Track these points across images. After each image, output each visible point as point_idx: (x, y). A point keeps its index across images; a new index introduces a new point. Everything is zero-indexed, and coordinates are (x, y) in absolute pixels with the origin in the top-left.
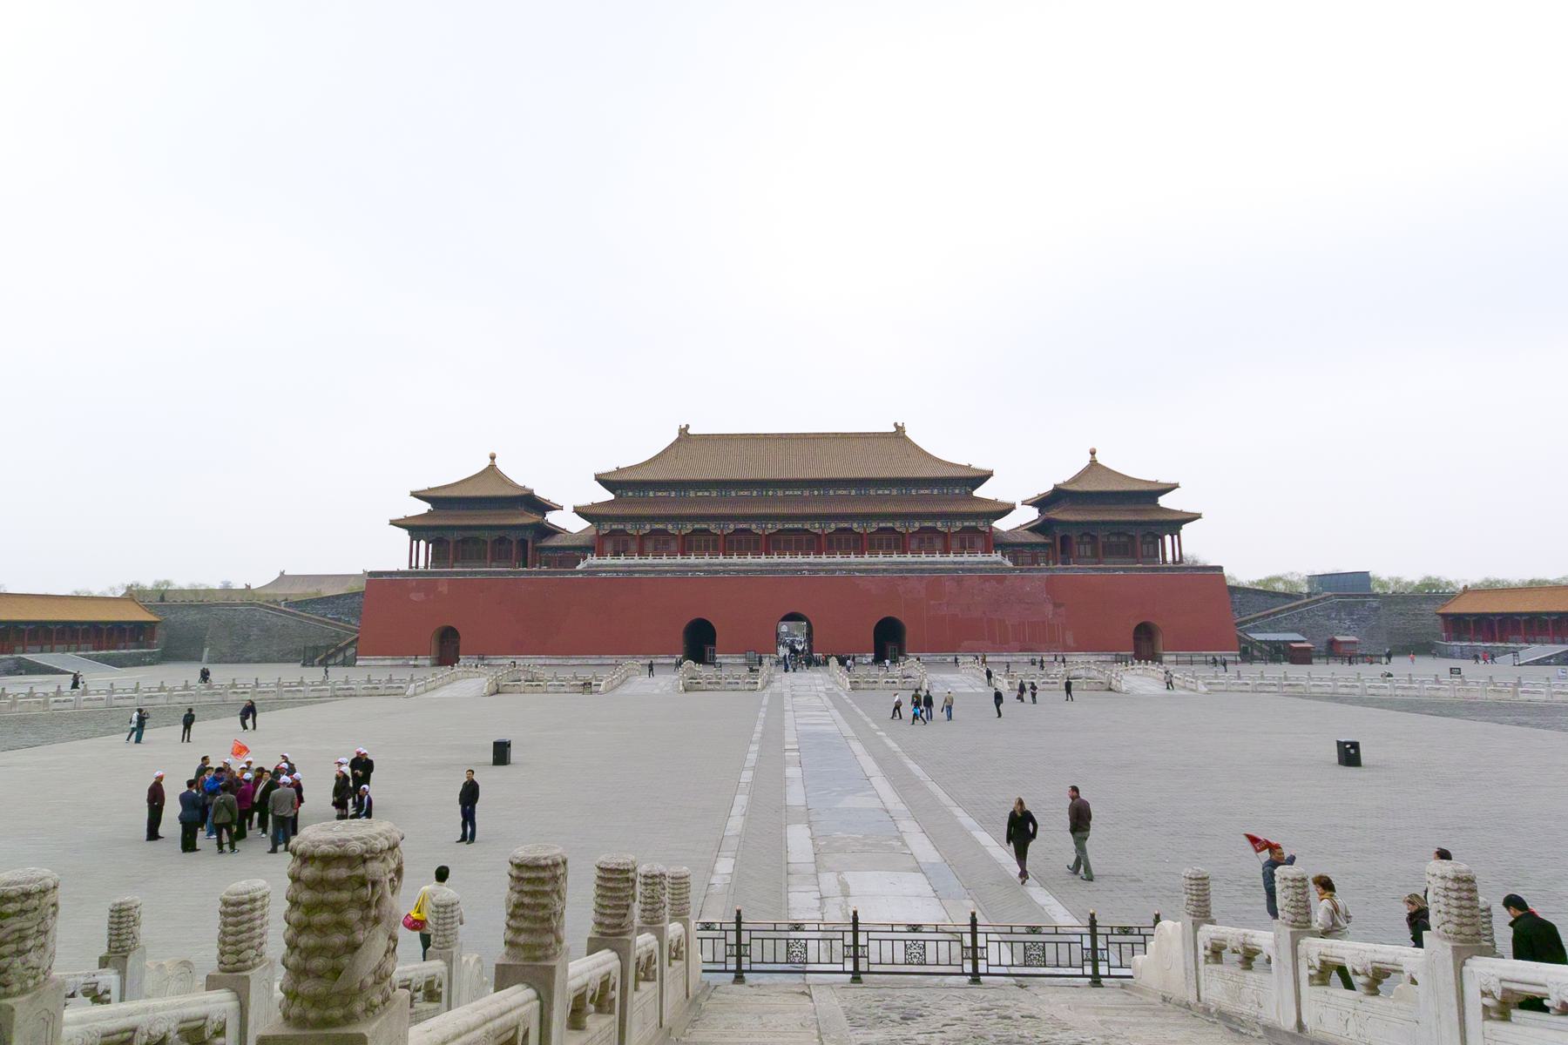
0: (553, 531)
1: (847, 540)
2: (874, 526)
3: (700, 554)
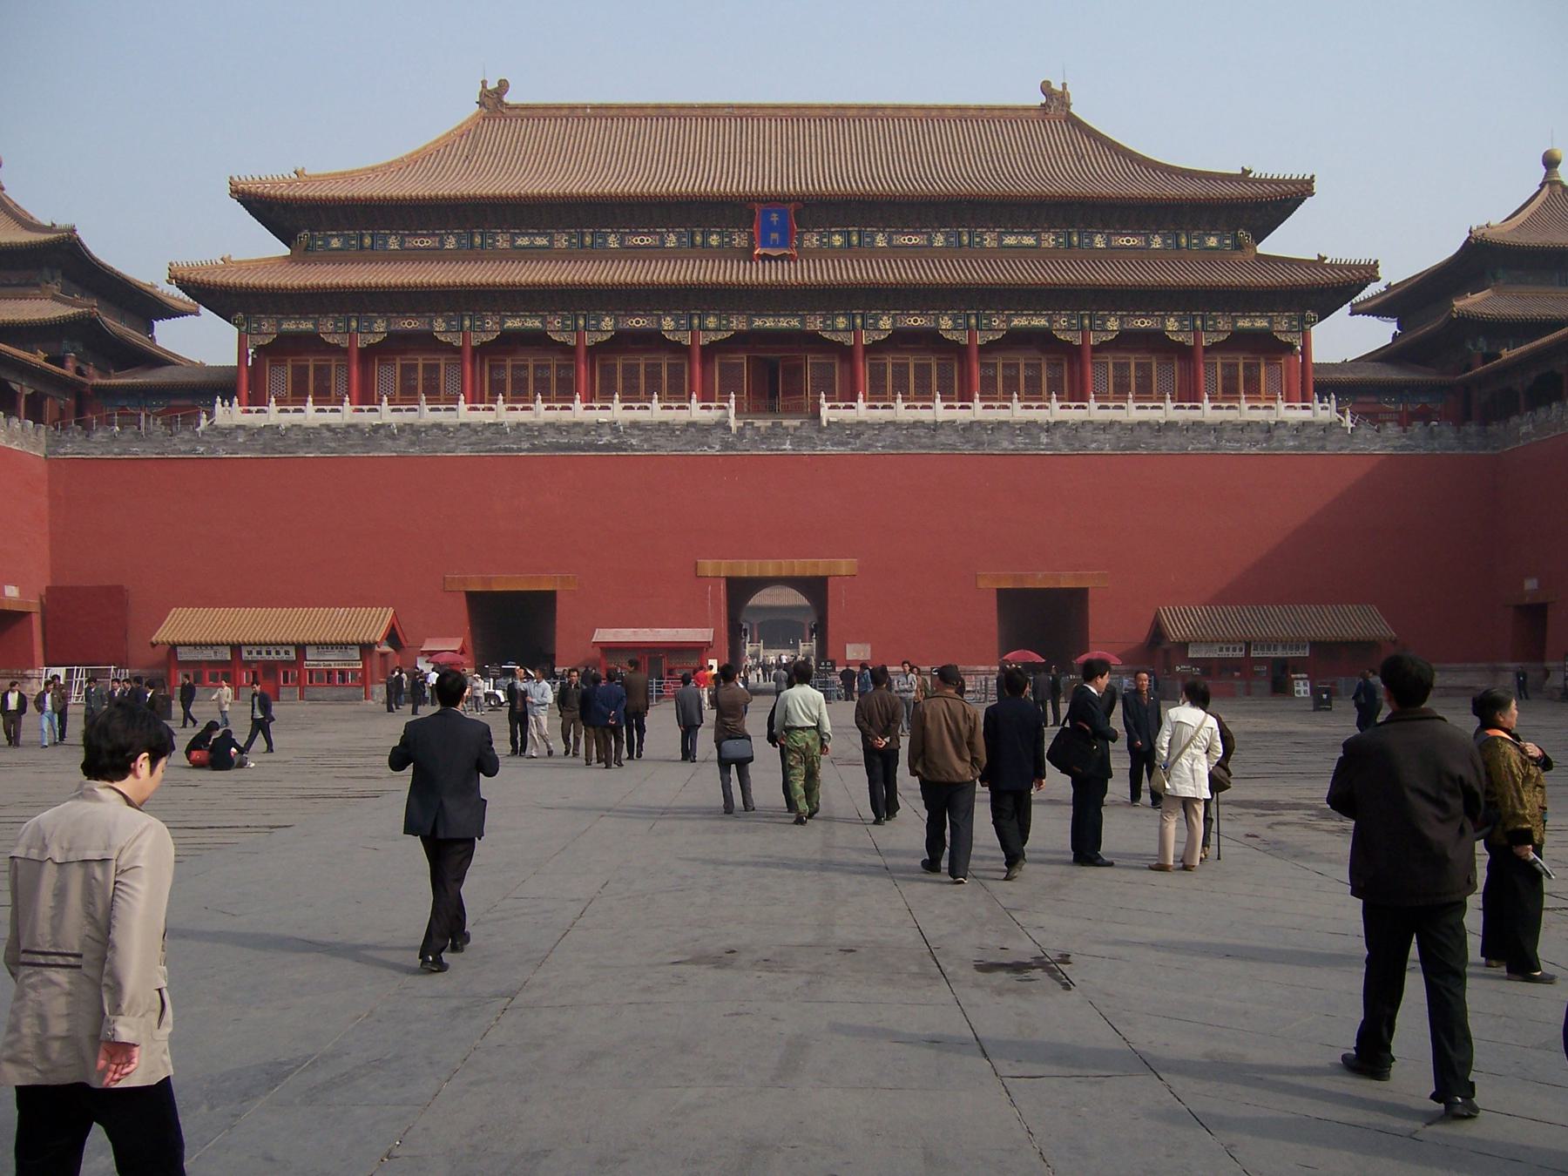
0: (159, 360)
1: (923, 372)
3: (520, 395)
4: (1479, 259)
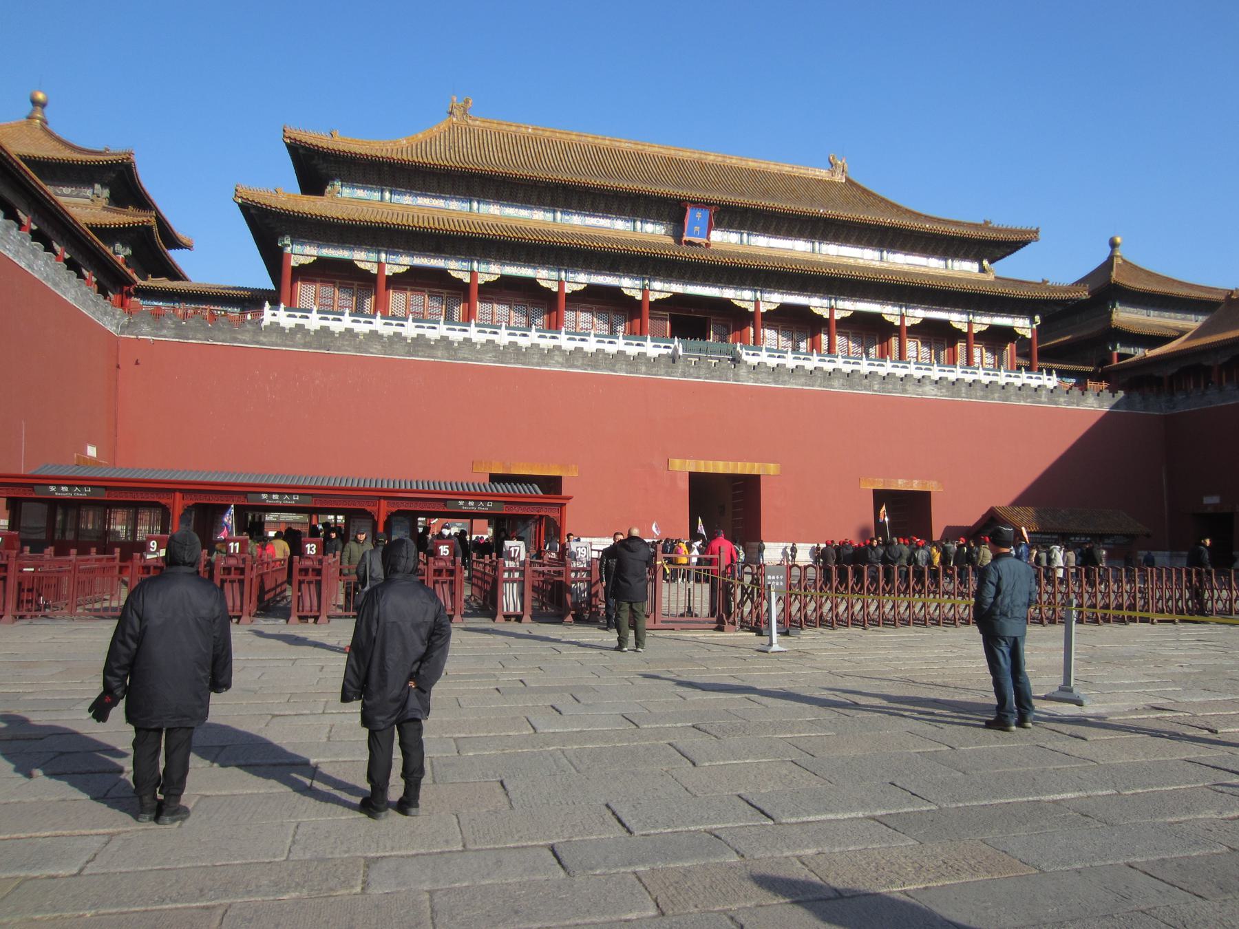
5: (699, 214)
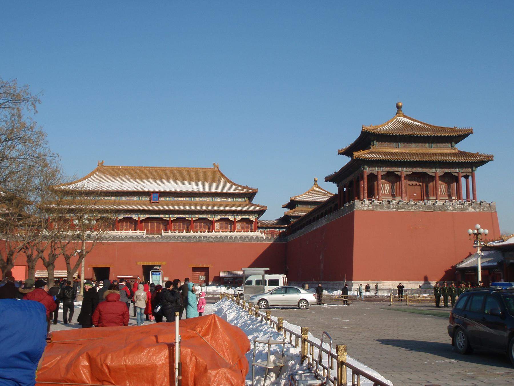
2: (196, 217)
4: (292, 205)
5: (155, 195)
